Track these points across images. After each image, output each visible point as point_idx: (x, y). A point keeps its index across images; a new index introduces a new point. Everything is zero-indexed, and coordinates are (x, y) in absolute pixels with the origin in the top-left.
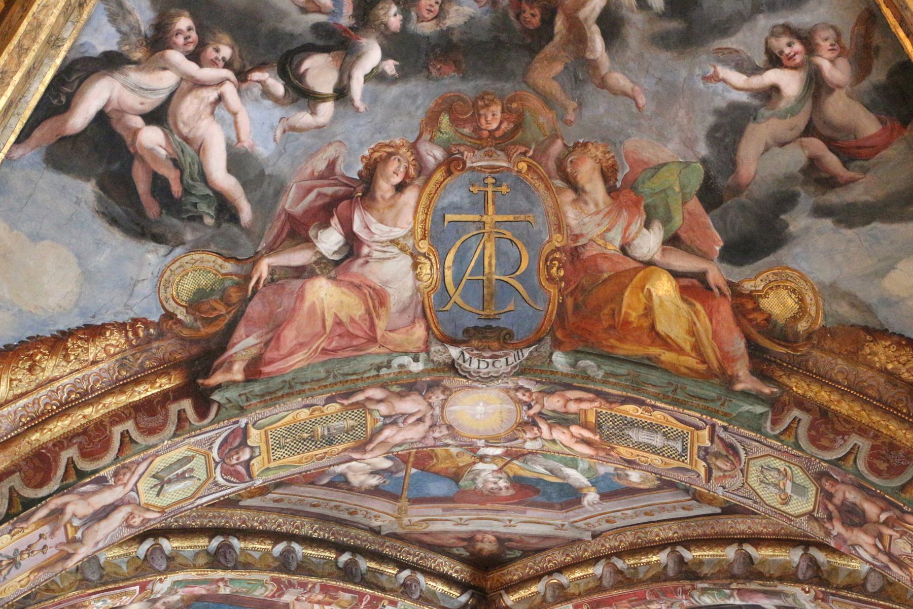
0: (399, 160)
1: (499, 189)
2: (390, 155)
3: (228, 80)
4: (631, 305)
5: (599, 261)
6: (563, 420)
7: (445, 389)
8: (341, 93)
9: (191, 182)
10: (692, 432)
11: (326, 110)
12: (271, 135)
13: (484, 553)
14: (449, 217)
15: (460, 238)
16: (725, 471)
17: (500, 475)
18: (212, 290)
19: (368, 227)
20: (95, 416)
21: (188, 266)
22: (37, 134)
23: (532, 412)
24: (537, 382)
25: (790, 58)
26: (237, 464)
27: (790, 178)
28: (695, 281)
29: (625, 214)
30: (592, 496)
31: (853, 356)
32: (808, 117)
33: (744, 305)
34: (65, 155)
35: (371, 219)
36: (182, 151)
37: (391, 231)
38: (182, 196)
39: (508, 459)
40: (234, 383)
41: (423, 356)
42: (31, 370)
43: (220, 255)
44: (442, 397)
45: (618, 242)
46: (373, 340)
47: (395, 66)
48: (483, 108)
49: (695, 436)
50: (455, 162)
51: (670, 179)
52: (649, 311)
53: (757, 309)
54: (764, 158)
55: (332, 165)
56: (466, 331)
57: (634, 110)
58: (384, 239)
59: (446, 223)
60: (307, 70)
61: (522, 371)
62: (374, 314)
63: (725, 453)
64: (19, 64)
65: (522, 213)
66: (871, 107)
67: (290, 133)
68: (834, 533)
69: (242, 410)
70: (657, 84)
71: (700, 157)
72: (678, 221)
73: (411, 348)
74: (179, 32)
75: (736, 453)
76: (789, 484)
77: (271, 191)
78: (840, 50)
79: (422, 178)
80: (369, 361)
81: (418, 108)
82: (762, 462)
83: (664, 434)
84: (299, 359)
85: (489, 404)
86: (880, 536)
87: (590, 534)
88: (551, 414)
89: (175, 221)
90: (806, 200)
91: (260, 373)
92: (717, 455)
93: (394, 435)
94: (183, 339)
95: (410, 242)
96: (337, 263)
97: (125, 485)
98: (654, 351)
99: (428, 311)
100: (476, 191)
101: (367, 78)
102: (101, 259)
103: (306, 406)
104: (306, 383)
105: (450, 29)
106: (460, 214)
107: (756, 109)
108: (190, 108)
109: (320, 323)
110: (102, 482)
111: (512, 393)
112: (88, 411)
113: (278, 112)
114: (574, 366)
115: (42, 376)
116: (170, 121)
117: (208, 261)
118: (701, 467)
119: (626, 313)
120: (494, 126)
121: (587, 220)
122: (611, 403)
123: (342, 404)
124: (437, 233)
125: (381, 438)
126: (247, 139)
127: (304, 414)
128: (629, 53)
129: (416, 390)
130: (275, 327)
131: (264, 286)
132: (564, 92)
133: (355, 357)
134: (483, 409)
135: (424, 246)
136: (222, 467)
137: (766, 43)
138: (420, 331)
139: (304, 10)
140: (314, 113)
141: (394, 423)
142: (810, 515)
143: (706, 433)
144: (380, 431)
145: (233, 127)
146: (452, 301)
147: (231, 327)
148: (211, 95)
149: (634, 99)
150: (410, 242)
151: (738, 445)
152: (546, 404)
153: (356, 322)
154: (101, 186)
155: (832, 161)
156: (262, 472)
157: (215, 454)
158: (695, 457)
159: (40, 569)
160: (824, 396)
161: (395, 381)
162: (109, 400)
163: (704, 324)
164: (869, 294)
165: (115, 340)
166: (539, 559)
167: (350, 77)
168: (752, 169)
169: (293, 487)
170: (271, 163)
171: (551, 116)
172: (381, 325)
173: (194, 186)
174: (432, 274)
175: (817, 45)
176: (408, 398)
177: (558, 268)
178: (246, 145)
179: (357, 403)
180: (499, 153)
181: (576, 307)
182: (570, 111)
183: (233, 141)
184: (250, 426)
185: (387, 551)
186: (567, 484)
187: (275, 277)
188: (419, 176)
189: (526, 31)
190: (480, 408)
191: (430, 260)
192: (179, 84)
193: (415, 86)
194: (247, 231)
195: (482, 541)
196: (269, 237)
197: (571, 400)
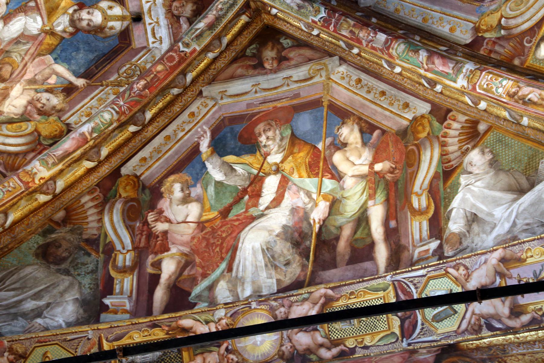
13: (270, 44)
17: (265, 150)
30: (204, 146)
39: (261, 174)
44: (284, 348)
68: (6, 354)
87: (204, 94)
94: (468, 357)
97: (473, 313)
103: (366, 347)
123: (345, 346)
127: (368, 341)
152: (217, 356)
156: (387, 288)
166: (233, 54)
169: (395, 128)
176: (305, 347)
184: (400, 338)
186: (221, 155)
195: (273, 59)
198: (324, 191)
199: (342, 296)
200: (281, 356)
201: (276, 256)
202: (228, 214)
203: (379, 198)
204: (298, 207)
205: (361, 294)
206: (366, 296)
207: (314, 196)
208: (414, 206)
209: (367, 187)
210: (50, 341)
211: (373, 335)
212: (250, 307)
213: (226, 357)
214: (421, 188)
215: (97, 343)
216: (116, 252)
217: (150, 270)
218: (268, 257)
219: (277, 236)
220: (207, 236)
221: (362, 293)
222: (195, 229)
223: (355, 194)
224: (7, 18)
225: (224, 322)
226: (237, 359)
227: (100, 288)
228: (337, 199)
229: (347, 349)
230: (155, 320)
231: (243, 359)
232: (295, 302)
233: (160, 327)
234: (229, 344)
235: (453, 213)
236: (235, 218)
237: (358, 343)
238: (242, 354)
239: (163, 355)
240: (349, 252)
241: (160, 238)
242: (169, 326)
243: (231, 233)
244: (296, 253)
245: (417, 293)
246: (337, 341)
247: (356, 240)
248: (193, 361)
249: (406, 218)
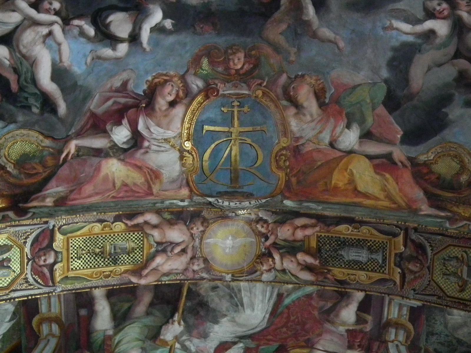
0: (172, 85)
1: (242, 109)
3: (57, 22)
4: (338, 179)
5: (315, 155)
7: (205, 222)
8: (134, 38)
9: (25, 84)
10: (390, 240)
11: (123, 48)
12: (84, 60)
14: (206, 127)
15: (214, 142)
16: (416, 273)
18: (34, 156)
19: (148, 128)
21: (18, 138)
23: (268, 243)
24: (273, 212)
25: (440, 12)
26: (44, 266)
27: (447, 85)
28: (384, 160)
29: (332, 120)
32: (455, 48)
35: (151, 123)
36: (21, 63)
37: (165, 132)
38: (17, 93)
43: (42, 134)
44: (201, 229)
45: (327, 141)
47: (172, 23)
48: (231, 54)
49: (393, 243)
50: (212, 90)
51: (364, 94)
52: (352, 181)
53: (431, 172)
55: (125, 84)
56: (220, 193)
57: (337, 51)
58: (160, 138)
59: (204, 131)
60: (111, 22)
62: (151, 183)
63: (415, 254)
65: (258, 125)
67: (97, 60)
69: (51, 215)
70: (351, 34)
71: (383, 78)
72: (370, 121)
76: (465, 268)
77: (81, 96)
79: (188, 99)
80: (147, 202)
81: (187, 52)
82: (444, 254)
83: (369, 249)
85: (236, 238)
88: (282, 243)
89: (11, 107)
90: (459, 98)
91: (66, 204)
92: (411, 259)
93: (163, 264)
94: (9, 183)
96: (125, 150)
99: (191, 183)
100: (225, 111)
101: (152, 30)
103: (101, 221)
104: (101, 207)
106: (215, 126)
108: (29, 38)
109: (111, 185)
111: (254, 225)
113: (89, 47)
116: (14, 44)
117: (33, 137)
119: (335, 183)
120: (239, 67)
121: (305, 126)
122: (329, 226)
123: (126, 224)
124: (199, 139)
125: (154, 265)
127: (97, 228)
128: (332, 15)
129: (182, 219)
130: (77, 184)
131: (72, 158)
132: (288, 42)
133: (137, 200)
134: (231, 242)
135: (188, 145)
136: (32, 265)
137: (424, 4)
138: (185, 192)
140: (114, 49)
141: (164, 251)
143: (401, 238)
144: (152, 258)
145: (58, 53)
146: (208, 179)
147: (46, 180)
148: (45, 31)
151: (426, 242)
152: (279, 234)
153: (138, 185)
156: (62, 279)
157: (27, 249)
158: (392, 265)
163: (392, 186)
167: (140, 28)
168: (420, 82)
170: (82, 78)
171: (278, 58)
172: (156, 189)
173: (27, 87)
174: (193, 164)
175: (458, 3)
176: (176, 227)
177: (285, 161)
178: (66, 64)
179: (137, 226)
180: (243, 84)
181: (299, 182)
182: (292, 55)
183: (57, 61)
184: (56, 229)
187: (80, 153)
188: (186, 97)
191: (192, 155)
192: (22, 21)
193: (185, 37)
194: (61, 120)
197: (298, 227)
198: (165, 349)
199: (120, 274)
200: (205, 222)
201: (228, 297)
202: (278, 348)
203: (99, 336)
204: (198, 338)
205: (96, 275)
206: (90, 273)
207: (177, 345)
208: (57, 326)
209: (113, 347)
210: (455, 302)
211: (90, 233)
212: (233, 276)
213: (269, 231)
214: (48, 341)
215: (406, 284)
216: (406, 344)
217: (369, 318)
218: (237, 298)
219: (225, 316)
220: (304, 333)
221: (95, 276)
222: (317, 342)
223: (128, 342)
225: (265, 267)
226: (258, 226)
227: (424, 317)
228: (150, 340)
229: (124, 221)
230: (340, 288)
231: (250, 225)
232: (179, 274)
233: (335, 279)
234: (263, 243)
235: (8, 318)
236: (271, 343)
237: (110, 226)
238: (251, 230)
239: (337, 250)
240: (138, 291)
241: (356, 344)
242: (326, 278)
243: (276, 329)
244: (203, 297)
245: (26, 274)
246: (135, 229)
247: (128, 301)
248: (306, 236)
249: (66, 316)
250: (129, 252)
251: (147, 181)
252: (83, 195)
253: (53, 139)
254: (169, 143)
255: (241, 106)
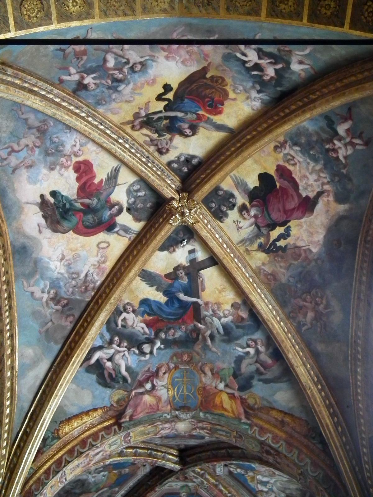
2: (162, 366)
4: (217, 401)
6: (203, 429)
8: (151, 353)
11: (148, 356)
14: (176, 380)
19: (157, 383)
20: (96, 430)
22: (84, 365)
25: (252, 346)
27: (252, 372)
31: (268, 414)
33: (243, 402)
34: (90, 369)
35: (158, 381)
40: (126, 421)
41: (170, 414)
42: (81, 420)
46: (158, 410)
51: (226, 372)
52: (221, 402)
53: (246, 402)
54: (247, 368)
55: (149, 369)
56: (180, 407)
61: (193, 417)
64: (81, 352)
66: (270, 357)
69: (129, 429)
72: (228, 380)
73: (167, 412)
74: (115, 340)
75: (242, 437)
78: (263, 344)
84: (141, 415)
86: (274, 457)
90: (256, 377)
91: (133, 419)
92: (238, 438)
94: (115, 410)
95: (166, 386)
96: (150, 391)
98: (223, 412)
101: (157, 349)
102: (97, 393)
105: (176, 338)
107: (245, 357)
108: (117, 357)
110: (98, 447)
112: (94, 429)
113: (137, 357)
114: (205, 416)
115: (84, 421)
118: (234, 440)
124: (173, 384)
126: (130, 364)
127: (143, 429)
130: (136, 407)
133: (154, 415)
135: (170, 387)
138: (169, 407)
139: (143, 335)
140: (145, 357)
142: (259, 452)
143: (235, 432)
147: (126, 407)
148: (122, 354)
149: (217, 353)
150: (167, 386)
154: (97, 376)
155: (262, 369)
157: (122, 439)
159: (83, 467)
160: (261, 423)
161: (164, 420)
162: (99, 426)
163: (234, 406)
164: (271, 399)
165: (100, 411)
172: (160, 406)
181: (205, 401)
185: (159, 449)
189: (193, 338)
190: (183, 425)
196: (135, 386)
200: (176, 422)
224: (268, 482)
250: (152, 432)
251: (157, 403)
252: (138, 413)
253: (127, 391)
254: (164, 388)
255: (187, 372)
